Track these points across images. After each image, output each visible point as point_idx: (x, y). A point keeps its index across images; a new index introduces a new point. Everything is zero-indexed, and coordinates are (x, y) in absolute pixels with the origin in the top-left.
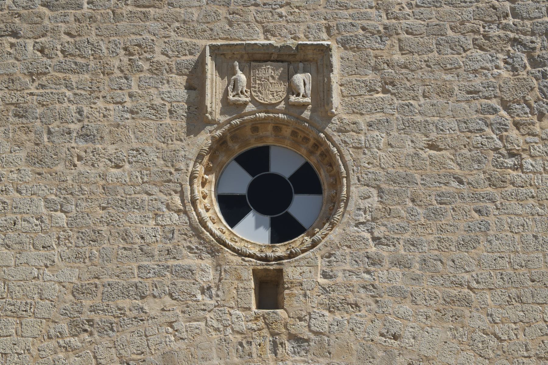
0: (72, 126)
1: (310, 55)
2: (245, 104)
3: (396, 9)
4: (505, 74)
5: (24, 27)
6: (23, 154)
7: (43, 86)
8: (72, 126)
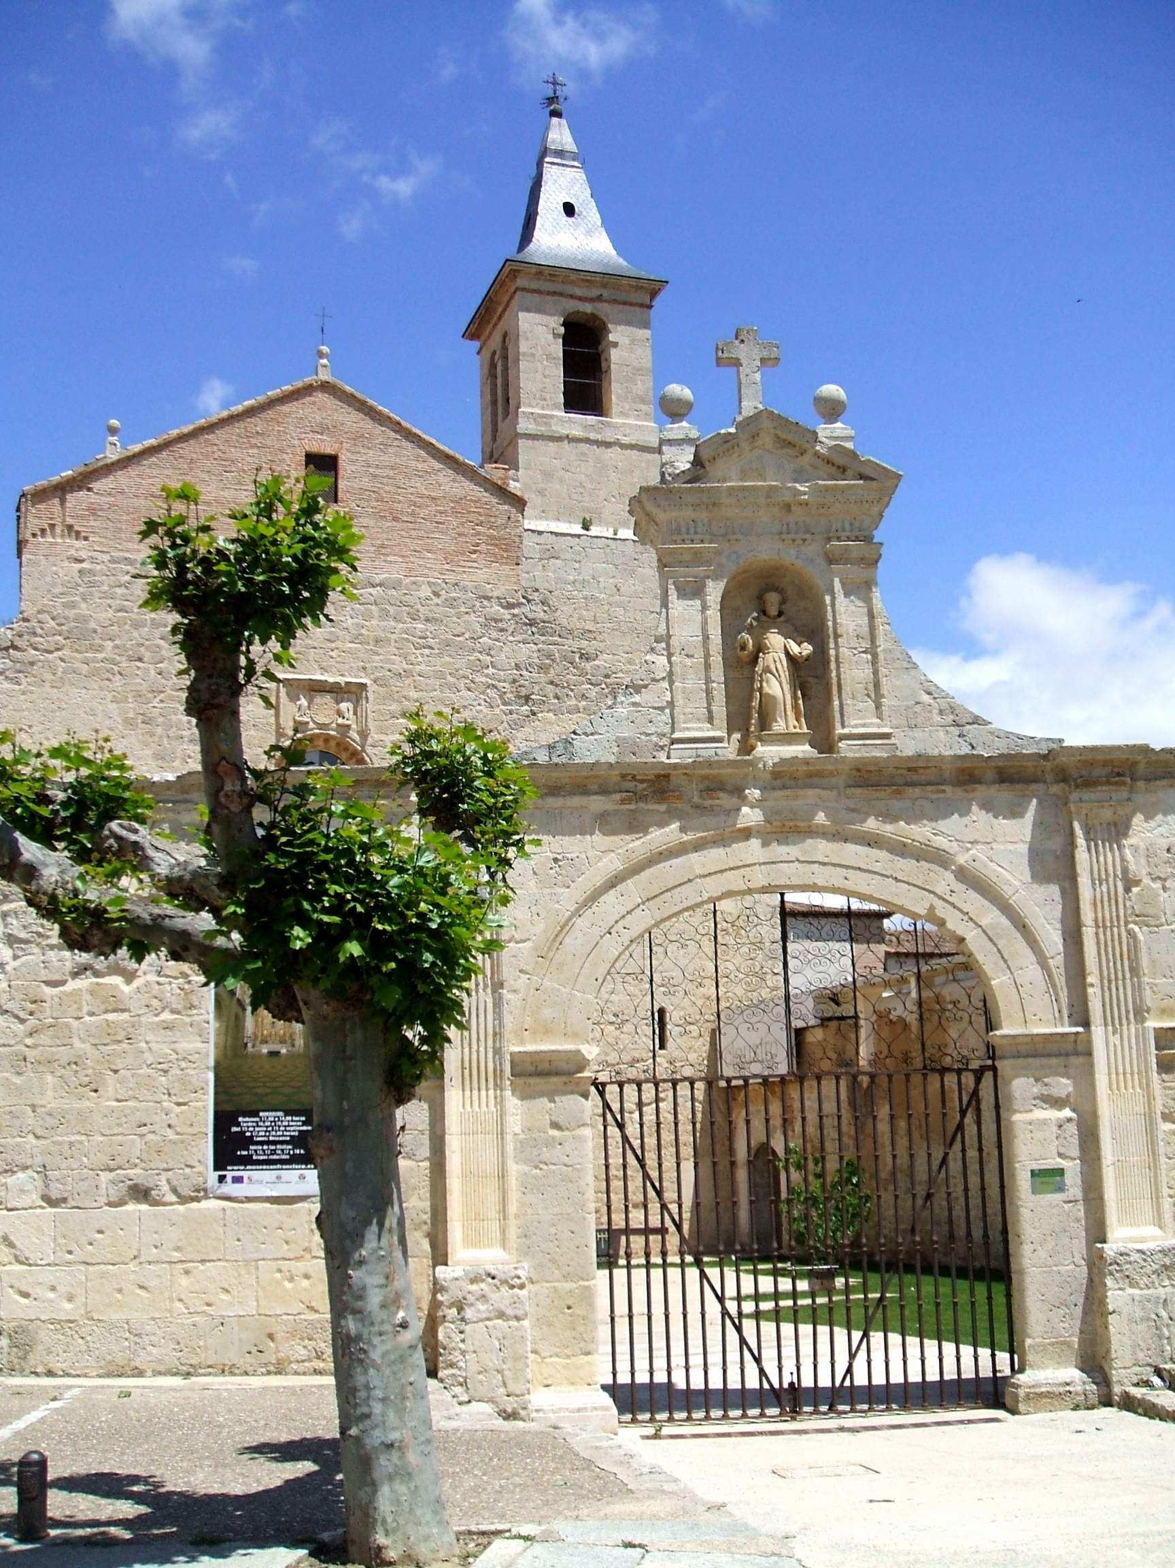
0: (184, 733)
1: (353, 689)
2: (307, 723)
3: (412, 658)
4: (485, 711)
5: (147, 656)
6: (149, 752)
7: (162, 701)
8: (184, 733)
